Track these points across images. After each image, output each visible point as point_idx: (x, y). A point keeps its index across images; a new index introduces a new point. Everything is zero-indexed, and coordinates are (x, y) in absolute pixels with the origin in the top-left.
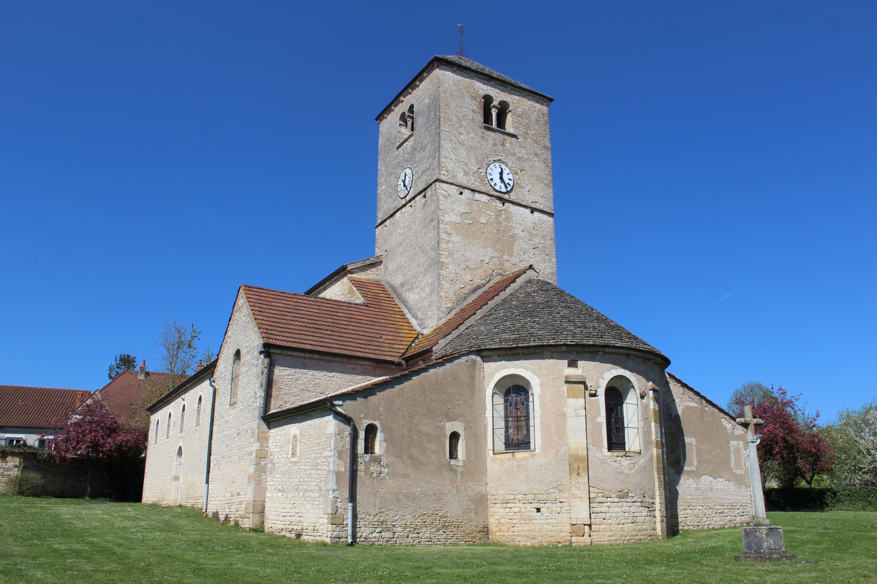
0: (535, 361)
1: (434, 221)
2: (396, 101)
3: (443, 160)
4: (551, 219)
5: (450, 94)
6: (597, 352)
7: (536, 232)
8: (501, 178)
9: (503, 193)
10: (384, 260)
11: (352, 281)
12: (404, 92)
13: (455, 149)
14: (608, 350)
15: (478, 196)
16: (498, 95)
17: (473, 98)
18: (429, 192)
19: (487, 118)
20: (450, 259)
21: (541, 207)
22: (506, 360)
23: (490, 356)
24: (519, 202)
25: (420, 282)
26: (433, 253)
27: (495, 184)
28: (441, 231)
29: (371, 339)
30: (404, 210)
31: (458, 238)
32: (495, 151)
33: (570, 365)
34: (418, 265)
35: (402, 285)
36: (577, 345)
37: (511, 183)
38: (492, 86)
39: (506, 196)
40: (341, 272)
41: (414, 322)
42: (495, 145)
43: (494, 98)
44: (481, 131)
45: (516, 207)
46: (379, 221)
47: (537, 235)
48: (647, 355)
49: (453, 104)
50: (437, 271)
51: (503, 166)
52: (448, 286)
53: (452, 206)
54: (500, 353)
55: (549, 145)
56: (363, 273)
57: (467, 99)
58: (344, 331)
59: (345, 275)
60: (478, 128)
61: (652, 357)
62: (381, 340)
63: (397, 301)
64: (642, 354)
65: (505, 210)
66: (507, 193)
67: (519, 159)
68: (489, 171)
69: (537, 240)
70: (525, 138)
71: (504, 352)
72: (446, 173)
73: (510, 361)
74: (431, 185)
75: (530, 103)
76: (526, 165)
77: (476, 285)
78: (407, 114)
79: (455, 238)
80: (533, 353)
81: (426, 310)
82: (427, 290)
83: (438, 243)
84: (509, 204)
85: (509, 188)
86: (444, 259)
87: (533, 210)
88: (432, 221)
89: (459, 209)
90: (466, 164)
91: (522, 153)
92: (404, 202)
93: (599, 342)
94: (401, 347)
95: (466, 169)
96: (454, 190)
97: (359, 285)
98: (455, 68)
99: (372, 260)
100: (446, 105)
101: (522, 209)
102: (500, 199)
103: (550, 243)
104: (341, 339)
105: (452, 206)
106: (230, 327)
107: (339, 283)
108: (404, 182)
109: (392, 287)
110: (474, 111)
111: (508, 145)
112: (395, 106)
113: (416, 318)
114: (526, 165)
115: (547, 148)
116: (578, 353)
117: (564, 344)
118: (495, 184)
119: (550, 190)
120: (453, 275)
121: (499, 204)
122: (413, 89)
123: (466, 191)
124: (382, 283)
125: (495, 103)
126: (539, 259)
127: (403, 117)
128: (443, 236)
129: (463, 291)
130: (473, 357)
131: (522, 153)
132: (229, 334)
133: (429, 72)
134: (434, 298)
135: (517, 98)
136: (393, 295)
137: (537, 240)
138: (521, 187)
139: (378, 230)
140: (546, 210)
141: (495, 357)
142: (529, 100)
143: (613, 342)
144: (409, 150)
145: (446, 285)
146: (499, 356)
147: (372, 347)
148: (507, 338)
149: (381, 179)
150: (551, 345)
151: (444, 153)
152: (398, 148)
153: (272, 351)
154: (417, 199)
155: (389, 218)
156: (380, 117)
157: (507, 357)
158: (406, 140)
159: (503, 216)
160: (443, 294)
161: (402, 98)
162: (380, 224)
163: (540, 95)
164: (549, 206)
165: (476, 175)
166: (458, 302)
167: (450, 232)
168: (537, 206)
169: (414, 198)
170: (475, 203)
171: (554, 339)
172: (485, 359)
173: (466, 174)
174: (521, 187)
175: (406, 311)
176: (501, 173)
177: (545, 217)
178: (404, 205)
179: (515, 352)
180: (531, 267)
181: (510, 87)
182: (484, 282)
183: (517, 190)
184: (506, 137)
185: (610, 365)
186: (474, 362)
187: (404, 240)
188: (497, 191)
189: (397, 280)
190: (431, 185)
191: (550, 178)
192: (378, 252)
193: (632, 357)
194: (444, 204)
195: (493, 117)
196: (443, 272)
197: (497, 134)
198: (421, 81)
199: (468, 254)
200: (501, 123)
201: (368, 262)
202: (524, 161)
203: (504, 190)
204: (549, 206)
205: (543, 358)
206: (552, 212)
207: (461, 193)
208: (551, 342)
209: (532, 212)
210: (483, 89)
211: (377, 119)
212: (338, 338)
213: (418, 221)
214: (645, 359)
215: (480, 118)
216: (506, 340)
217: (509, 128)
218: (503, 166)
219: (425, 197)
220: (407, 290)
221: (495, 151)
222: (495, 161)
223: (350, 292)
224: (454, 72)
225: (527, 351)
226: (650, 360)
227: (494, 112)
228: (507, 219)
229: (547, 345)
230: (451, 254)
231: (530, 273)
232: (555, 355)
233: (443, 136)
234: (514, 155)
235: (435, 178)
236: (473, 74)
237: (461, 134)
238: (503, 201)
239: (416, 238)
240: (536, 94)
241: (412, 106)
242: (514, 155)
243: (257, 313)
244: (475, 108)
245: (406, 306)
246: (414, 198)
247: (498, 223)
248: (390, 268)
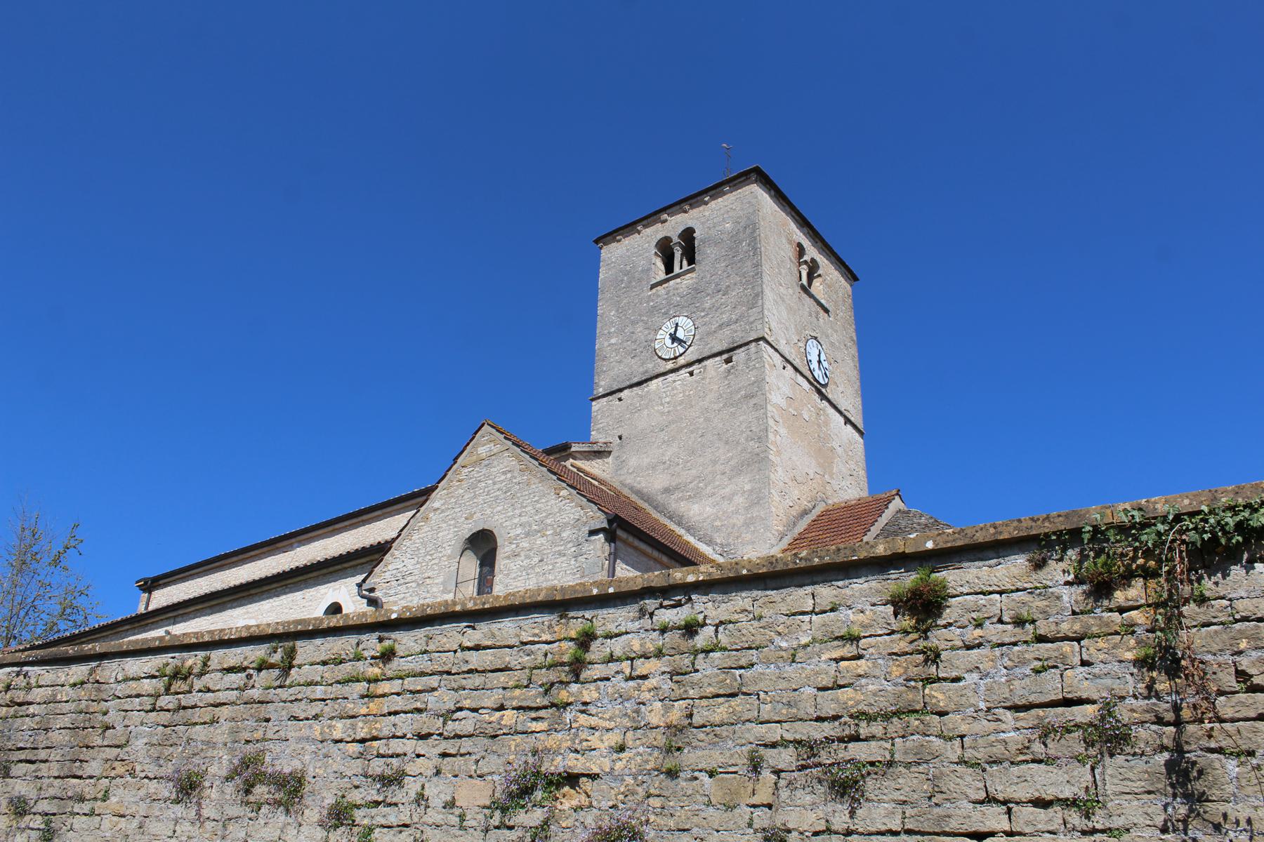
1: (755, 395)
18: (739, 356)
30: (671, 377)
46: (601, 391)
75: (836, 273)
79: (783, 431)
82: (739, 500)
92: (670, 365)
96: (778, 360)
112: (645, 227)
113: (710, 542)
119: (859, 399)
122: (692, 207)
123: (789, 367)
136: (645, 505)
153: (620, 533)
155: (631, 386)
162: (604, 396)
169: (700, 361)
177: (857, 435)
181: (820, 244)
189: (655, 483)
198: (713, 198)
211: (597, 242)
235: (753, 336)
239: (707, 420)
245: (679, 524)
248: (633, 462)
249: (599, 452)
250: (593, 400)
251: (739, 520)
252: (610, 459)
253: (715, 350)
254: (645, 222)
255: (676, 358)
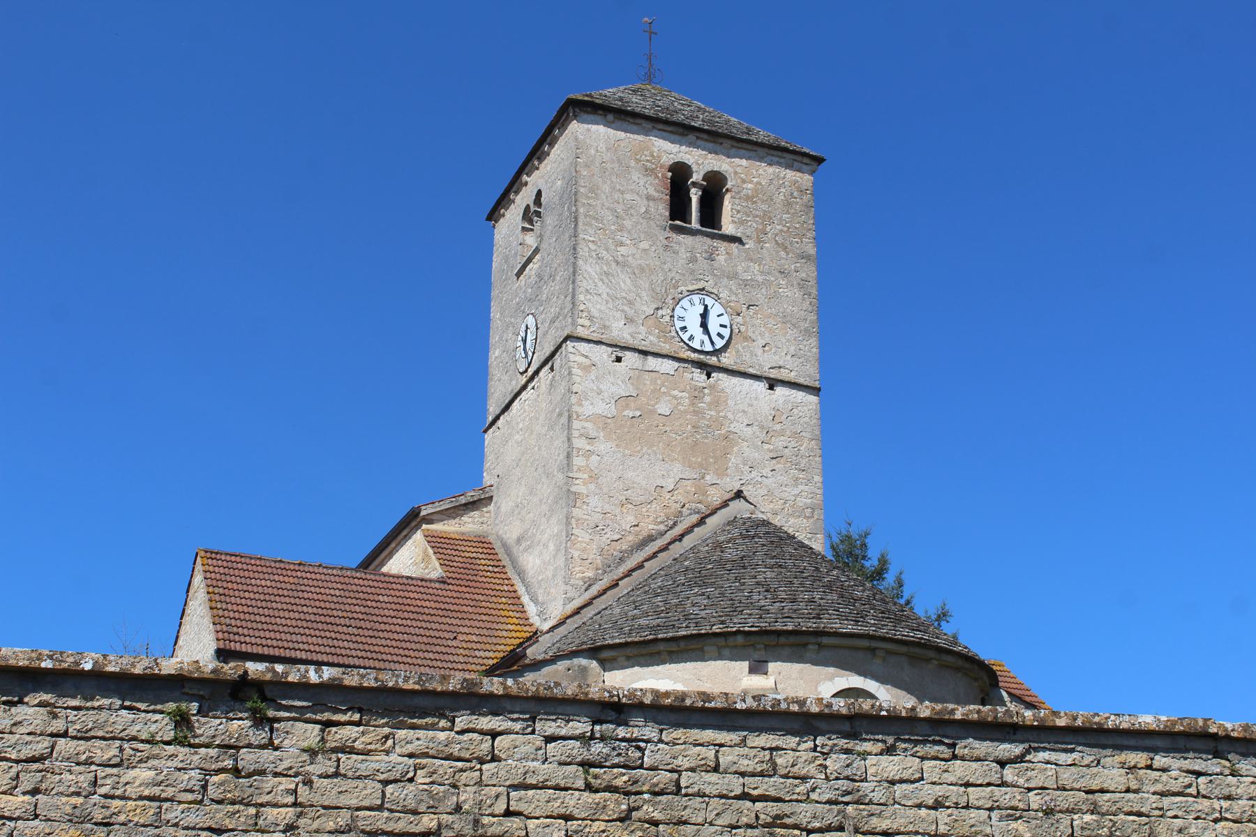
0: (690, 666)
2: (515, 184)
3: (582, 297)
4: (813, 399)
5: (607, 168)
6: (805, 645)
7: (778, 427)
8: (704, 325)
9: (707, 353)
10: (494, 494)
11: (433, 540)
12: (526, 166)
13: (607, 274)
14: (825, 640)
15: (652, 362)
16: (701, 161)
17: (648, 171)
18: (557, 360)
19: (678, 209)
20: (592, 487)
21: (792, 376)
22: (642, 665)
23: (614, 659)
24: (742, 369)
25: (543, 532)
26: (560, 476)
27: (691, 338)
28: (576, 434)
29: (434, 641)
30: (524, 395)
31: (609, 445)
32: (692, 272)
33: (753, 670)
34: (541, 501)
35: (519, 541)
36: (763, 633)
37: (726, 333)
38: (690, 145)
39: (713, 360)
40: (410, 521)
41: (531, 609)
42: (693, 260)
43: (694, 168)
44: (662, 235)
45: (736, 380)
46: (490, 419)
47: (782, 433)
48: (918, 650)
49: (606, 188)
50: (565, 510)
51: (709, 301)
52: (587, 537)
53: (598, 383)
54: (628, 651)
55: (811, 250)
56: (453, 522)
57: (635, 176)
58: (383, 627)
59: (418, 527)
60: (657, 231)
61: (931, 654)
62: (454, 643)
63: (511, 573)
64: (904, 649)
65: (712, 387)
66: (716, 352)
67: (746, 283)
68: (679, 311)
69: (779, 442)
70: (759, 241)
71: (634, 651)
72: (587, 323)
73: (647, 666)
74: (560, 346)
75: (771, 170)
76: (760, 296)
77: (645, 534)
78: (533, 208)
79: (603, 447)
80: (687, 651)
81: (549, 587)
82: (552, 547)
83: (568, 456)
84: (721, 375)
85: (720, 343)
86: (579, 487)
87: (772, 384)
88: (560, 415)
89: (614, 389)
90: (630, 303)
91: (753, 271)
92: (524, 380)
93: (811, 625)
94: (491, 654)
95: (630, 312)
96: (602, 355)
97: (439, 544)
98: (610, 117)
99: (471, 495)
100: (592, 190)
101: (748, 381)
102: (701, 365)
103: (809, 446)
104: (374, 641)
105: (598, 383)
106: (183, 627)
107: (410, 542)
108: (524, 341)
109: (504, 545)
110: (649, 198)
111: (721, 259)
112: (517, 193)
113: (534, 600)
114: (760, 296)
115: (804, 256)
116: (766, 647)
117: (738, 632)
118: (691, 338)
119: (813, 341)
120: (597, 518)
121: (699, 376)
122: (541, 160)
123: (629, 356)
124: (491, 539)
125: (697, 177)
126: (783, 479)
127: (528, 216)
128: (579, 443)
129: (618, 546)
130: (583, 662)
131: (753, 271)
132: (180, 642)
133: (563, 127)
134: (561, 562)
135: (744, 162)
136: (506, 561)
137: (779, 442)
138: (746, 339)
139: (488, 437)
140: (801, 381)
141: (622, 660)
142: (770, 164)
143: (836, 625)
144: (533, 279)
145: (582, 535)
146: (628, 658)
147: (431, 655)
148: (645, 625)
149: (494, 338)
150: (715, 634)
151: (584, 284)
152: (519, 274)
154: (542, 374)
156: (494, 215)
157: (642, 660)
158: (529, 261)
159: (707, 399)
160: (576, 554)
161: (525, 178)
163: (794, 152)
164: (808, 372)
165: (651, 321)
166: (607, 568)
167: (593, 434)
168: (784, 375)
169: (537, 372)
170: (647, 376)
171: (722, 622)
172: (606, 665)
173: (629, 321)
174: (746, 339)
175: (521, 590)
176: (704, 316)
177: (800, 395)
178: (524, 387)
179: (653, 649)
180: (739, 495)
181: (727, 143)
182: (662, 527)
183: (737, 345)
184: (716, 243)
185: (831, 670)
186: (584, 670)
187: (523, 453)
188: (695, 351)
189: (510, 532)
190: (560, 346)
191: (813, 317)
192: (488, 479)
193: (878, 652)
194: (582, 382)
195: (693, 205)
196: (576, 512)
197: (699, 238)
198: (552, 145)
199: (630, 474)
200: (711, 216)
201: (463, 500)
202: (760, 289)
203: (708, 348)
204: (808, 372)
205: (703, 659)
206: (817, 384)
207: (619, 360)
208: (716, 629)
209: (771, 388)
210: (669, 151)
212: (369, 640)
213: (542, 417)
214: (913, 659)
215: (662, 210)
216: (641, 628)
217: (728, 227)
218: (709, 301)
219: (552, 369)
220: (526, 550)
221: (692, 272)
222: (692, 292)
223: (426, 559)
224: (608, 124)
225: (673, 647)
226: (929, 660)
227: (695, 196)
228: (716, 403)
229: (707, 634)
230: (594, 478)
231: (737, 507)
232: (726, 652)
233: (583, 251)
234: (733, 276)
236: (648, 125)
237: (622, 244)
238: (708, 369)
240: (785, 150)
241: (539, 193)
242: (733, 276)
243: (217, 597)
244: (652, 191)
245: (523, 581)
246: (537, 372)
247: (696, 413)
248: (503, 509)
249: (474, 503)
250: (485, 431)
251: (550, 574)
252: (491, 507)
253: (547, 355)
254: (514, 189)
255: (526, 371)
